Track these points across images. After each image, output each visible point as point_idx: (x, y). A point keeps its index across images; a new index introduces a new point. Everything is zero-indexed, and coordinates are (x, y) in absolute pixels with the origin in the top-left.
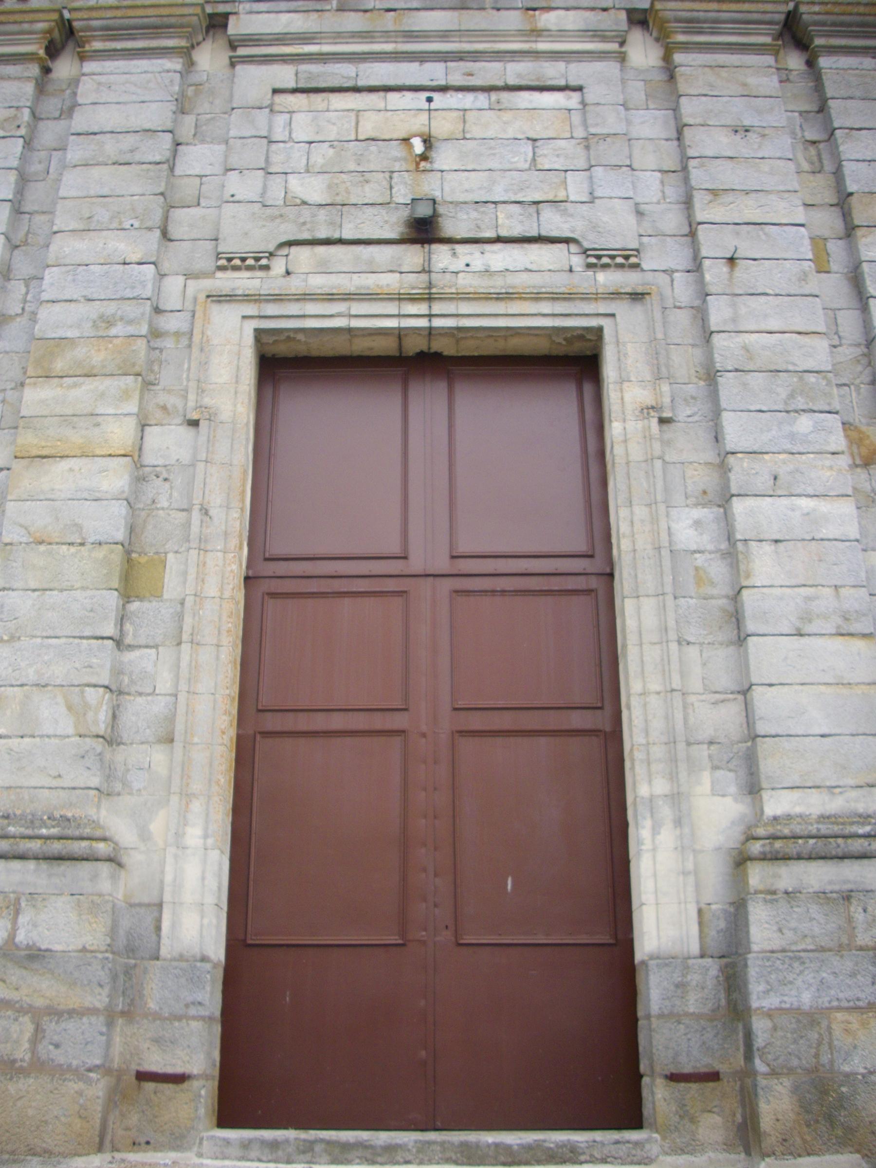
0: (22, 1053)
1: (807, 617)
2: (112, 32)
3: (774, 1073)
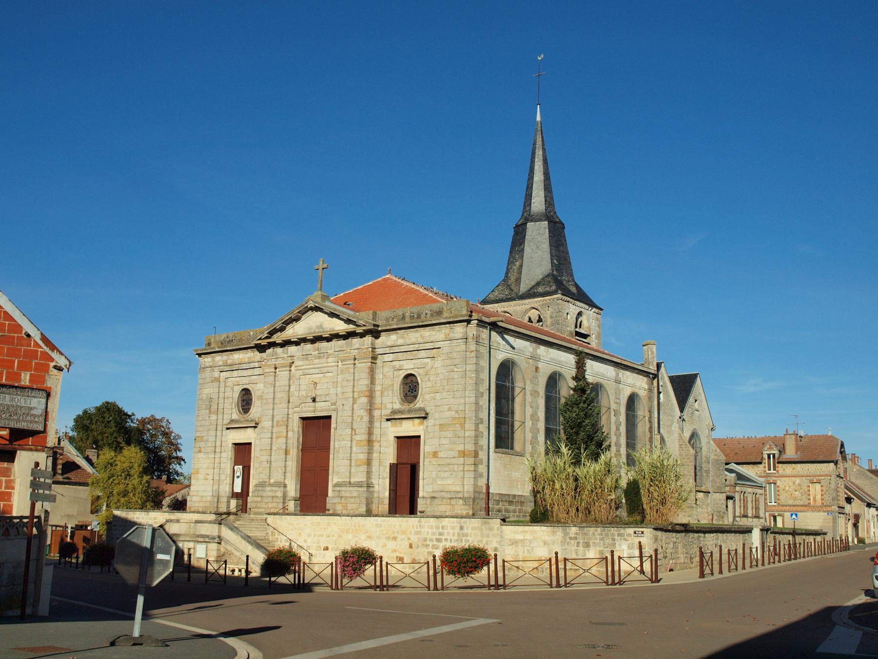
0: (276, 507)
1: (344, 457)
2: (281, 367)
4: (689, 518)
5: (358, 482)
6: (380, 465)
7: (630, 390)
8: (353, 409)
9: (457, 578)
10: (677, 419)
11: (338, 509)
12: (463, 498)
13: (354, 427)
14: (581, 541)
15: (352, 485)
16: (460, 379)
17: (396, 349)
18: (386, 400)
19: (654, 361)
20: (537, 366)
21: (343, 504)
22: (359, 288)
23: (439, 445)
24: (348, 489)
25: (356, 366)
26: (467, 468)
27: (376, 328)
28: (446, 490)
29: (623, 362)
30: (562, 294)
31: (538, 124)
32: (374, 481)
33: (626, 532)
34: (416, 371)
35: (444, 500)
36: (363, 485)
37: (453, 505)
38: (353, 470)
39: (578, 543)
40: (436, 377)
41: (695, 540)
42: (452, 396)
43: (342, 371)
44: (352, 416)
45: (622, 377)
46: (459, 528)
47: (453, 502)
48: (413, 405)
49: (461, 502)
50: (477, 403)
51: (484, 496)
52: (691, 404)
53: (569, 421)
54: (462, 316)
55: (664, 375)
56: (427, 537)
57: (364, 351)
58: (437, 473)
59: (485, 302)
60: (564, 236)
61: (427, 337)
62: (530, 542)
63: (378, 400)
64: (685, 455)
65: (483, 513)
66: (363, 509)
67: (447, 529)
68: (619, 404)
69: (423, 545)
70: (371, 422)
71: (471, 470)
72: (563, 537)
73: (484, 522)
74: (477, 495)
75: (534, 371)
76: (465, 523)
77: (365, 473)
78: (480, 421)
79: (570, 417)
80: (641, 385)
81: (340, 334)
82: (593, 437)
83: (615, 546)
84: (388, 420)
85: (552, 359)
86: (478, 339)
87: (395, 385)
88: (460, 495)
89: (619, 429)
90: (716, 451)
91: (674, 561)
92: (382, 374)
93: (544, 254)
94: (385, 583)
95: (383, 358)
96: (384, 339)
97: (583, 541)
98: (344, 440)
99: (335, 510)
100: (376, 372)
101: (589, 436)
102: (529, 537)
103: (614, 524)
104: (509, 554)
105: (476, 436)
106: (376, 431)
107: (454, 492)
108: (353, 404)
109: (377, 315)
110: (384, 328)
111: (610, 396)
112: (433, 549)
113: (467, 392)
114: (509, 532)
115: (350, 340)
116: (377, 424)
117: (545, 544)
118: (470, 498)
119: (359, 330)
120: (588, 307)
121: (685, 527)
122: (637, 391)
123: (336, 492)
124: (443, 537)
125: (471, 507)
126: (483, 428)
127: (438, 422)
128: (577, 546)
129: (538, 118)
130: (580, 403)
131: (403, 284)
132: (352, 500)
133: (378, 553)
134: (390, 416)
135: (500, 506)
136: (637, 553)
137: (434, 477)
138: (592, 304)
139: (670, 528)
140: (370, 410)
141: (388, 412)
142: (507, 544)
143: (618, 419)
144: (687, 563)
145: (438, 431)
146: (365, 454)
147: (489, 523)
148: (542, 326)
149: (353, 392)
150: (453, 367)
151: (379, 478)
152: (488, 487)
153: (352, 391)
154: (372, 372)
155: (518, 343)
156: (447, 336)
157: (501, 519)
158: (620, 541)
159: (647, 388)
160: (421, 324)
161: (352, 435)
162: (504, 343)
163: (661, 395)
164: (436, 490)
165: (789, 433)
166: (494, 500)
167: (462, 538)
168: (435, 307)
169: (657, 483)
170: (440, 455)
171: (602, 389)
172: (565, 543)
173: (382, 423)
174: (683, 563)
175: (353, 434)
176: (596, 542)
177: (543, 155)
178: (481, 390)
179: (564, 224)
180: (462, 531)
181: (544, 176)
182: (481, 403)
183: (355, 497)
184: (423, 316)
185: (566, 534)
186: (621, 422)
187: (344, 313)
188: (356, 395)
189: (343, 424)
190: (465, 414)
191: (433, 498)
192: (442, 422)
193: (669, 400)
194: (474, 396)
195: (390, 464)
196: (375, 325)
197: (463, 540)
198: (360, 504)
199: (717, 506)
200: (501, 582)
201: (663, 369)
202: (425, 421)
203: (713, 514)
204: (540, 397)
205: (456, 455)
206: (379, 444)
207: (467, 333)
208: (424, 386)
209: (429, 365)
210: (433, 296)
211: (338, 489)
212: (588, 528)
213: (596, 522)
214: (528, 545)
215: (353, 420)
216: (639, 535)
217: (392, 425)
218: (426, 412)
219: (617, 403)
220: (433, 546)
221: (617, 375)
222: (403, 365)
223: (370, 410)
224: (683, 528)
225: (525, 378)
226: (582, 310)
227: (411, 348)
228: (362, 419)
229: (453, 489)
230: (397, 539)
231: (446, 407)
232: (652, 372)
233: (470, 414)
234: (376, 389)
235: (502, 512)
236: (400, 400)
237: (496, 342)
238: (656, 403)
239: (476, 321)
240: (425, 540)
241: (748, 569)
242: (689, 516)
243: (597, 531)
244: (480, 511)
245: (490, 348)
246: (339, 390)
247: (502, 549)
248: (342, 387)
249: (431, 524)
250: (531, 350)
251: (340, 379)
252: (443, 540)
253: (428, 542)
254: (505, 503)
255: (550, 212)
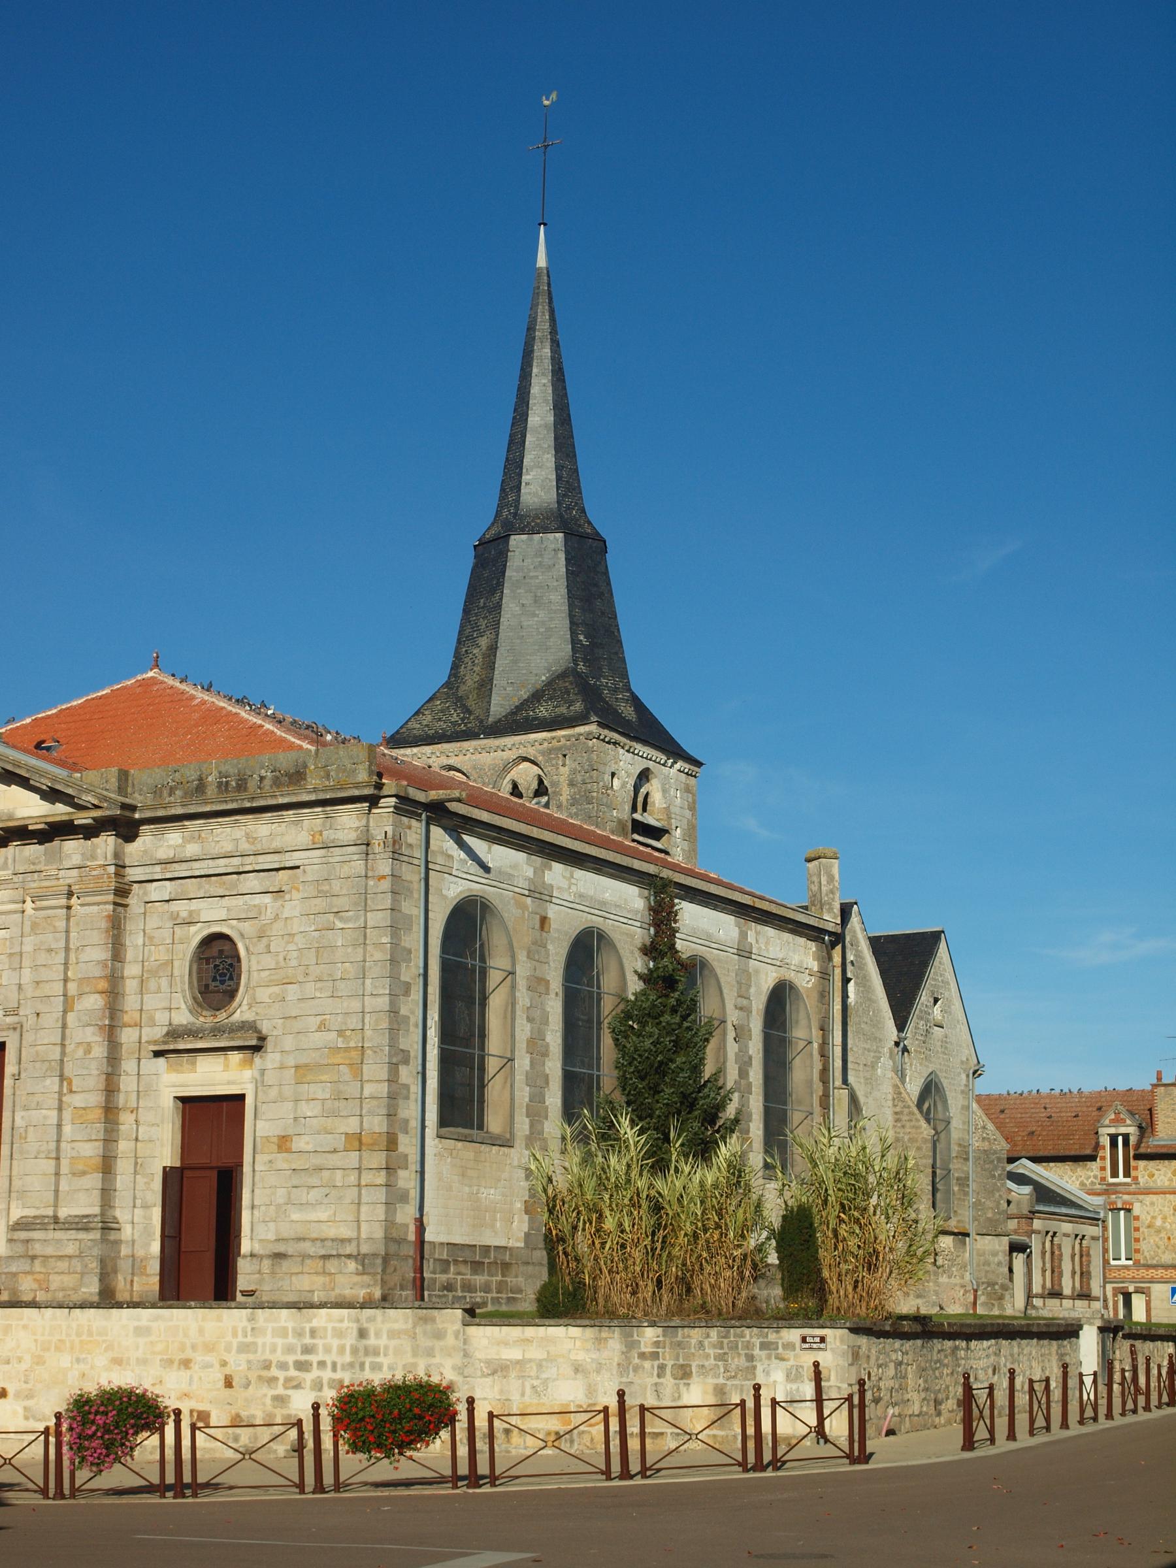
3: (5, 1289)
4: (919, 1301)
5: (76, 1216)
6: (136, 1173)
7: (775, 975)
8: (64, 1026)
9: (373, 1460)
10: (890, 1049)
11: (22, 1288)
12: (358, 1257)
13: (67, 1073)
14: (670, 1363)
15: (61, 1226)
16: (350, 950)
17: (181, 870)
18: (152, 1002)
19: (833, 900)
20: (544, 914)
21: (36, 1276)
22: (75, 703)
23: (295, 1119)
24: (51, 1235)
25: (73, 911)
26: (366, 1178)
27: (128, 814)
28: (314, 1235)
29: (760, 904)
30: (600, 724)
31: (539, 275)
32: (121, 1214)
33: (781, 1338)
34: (232, 927)
35: (308, 1262)
36: (92, 1225)
37: (330, 1274)
38: (64, 1186)
39: (662, 1368)
40: (288, 943)
41: (946, 1357)
42: (330, 994)
43: (34, 926)
44: (63, 1045)
45: (754, 942)
46: (355, 1333)
47: (332, 1266)
48: (224, 1015)
49: (352, 1266)
50: (394, 1011)
51: (410, 1251)
52: (924, 1008)
53: (634, 1059)
54: (357, 786)
55: (858, 933)
56: (271, 1357)
57: (94, 873)
58: (289, 1193)
59: (397, 740)
60: (606, 573)
61: (264, 840)
62: (540, 1366)
63: (131, 1002)
64: (910, 1139)
65: (409, 1293)
66: (91, 1288)
67: (325, 1337)
68: (745, 1010)
69: (260, 1378)
70: (113, 1058)
71: (378, 1183)
72: (623, 1353)
73: (420, 1319)
74: (393, 1248)
75: (537, 926)
76: (371, 1319)
77: (97, 1194)
78: (400, 1057)
79: (636, 1050)
80: (801, 962)
81: (30, 828)
82: (696, 1099)
83: (754, 1374)
84: (158, 1054)
85: (581, 896)
86: (397, 847)
87: (176, 964)
88: (349, 1249)
89: (748, 1074)
90: (984, 1127)
91: (897, 1410)
92: (142, 933)
93: (551, 619)
94: (187, 1478)
95: (145, 894)
96: (146, 842)
97: (672, 1362)
98: (38, 1106)
99: (14, 1292)
100: (128, 928)
101: (684, 1096)
102: (535, 1353)
103: (751, 1319)
104: (485, 1399)
105: (392, 1097)
106: (127, 1084)
107: (333, 1240)
108: (65, 1012)
109: (130, 778)
110: (148, 814)
111: (725, 991)
112: (286, 1388)
113: (368, 982)
114: (485, 1342)
115: (56, 843)
116: (128, 1065)
117: (577, 1371)
118: (375, 1255)
119: (83, 819)
120: (664, 758)
121: (923, 1325)
122: (791, 976)
123: (19, 1244)
124: (313, 1359)
125: (379, 1277)
126: (407, 1075)
127: (291, 1061)
128: (659, 1376)
129: (542, 261)
130: (662, 1013)
131: (193, 697)
132: (63, 1265)
133: (170, 1402)
134: (165, 1043)
135: (451, 1276)
136: (809, 1391)
137: (281, 1201)
138: (674, 751)
139: (888, 1328)
140: (112, 1028)
141: (159, 1032)
142: (479, 1373)
143: (743, 1050)
144: (926, 1413)
145: (293, 1082)
146: (97, 1144)
147: (433, 1320)
148: (547, 806)
149: (66, 980)
150: (331, 917)
151: (134, 1207)
152: (421, 1228)
153: (62, 977)
154: (116, 928)
155: (498, 855)
156: (317, 836)
157: (465, 1310)
158: (767, 1362)
159: (816, 969)
160: (248, 805)
161: (61, 1093)
162: (463, 855)
163: (851, 987)
164: (285, 1235)
165: (1165, 1081)
166: (435, 1260)
167: (362, 1359)
168: (285, 760)
169: (856, 1214)
170: (300, 1144)
171: (706, 972)
172: (628, 1368)
173: (143, 1061)
174: (918, 1416)
175: (65, 1091)
176: (706, 1363)
177: (553, 358)
178: (405, 977)
179: (605, 542)
180: (364, 1342)
181: (555, 415)
182: (403, 1011)
183: (70, 1257)
184: (252, 784)
185: (631, 1345)
186: (750, 1058)
187: (42, 773)
188: (72, 988)
189: (38, 1065)
190: (363, 1038)
191: (279, 1256)
192: (303, 1060)
193: (870, 1000)
194: (388, 992)
195: (165, 1168)
196: (124, 806)
197: (367, 1366)
198: (82, 1274)
199: (987, 1268)
200: (483, 1468)
201: (855, 920)
202: (257, 1059)
203: (976, 1291)
204: (552, 995)
205: (340, 1142)
206: (133, 1117)
207: (368, 830)
208: (254, 967)
209: (269, 910)
210: (276, 730)
211: (23, 1235)
212: (686, 1330)
213: (707, 1315)
214: (533, 1373)
215: (63, 1053)
216: (815, 1346)
217: (171, 1069)
218: (259, 1032)
219: (741, 1009)
220: (288, 1380)
221: (743, 935)
222: (198, 912)
223: (112, 1028)
224: (918, 1328)
225: (515, 944)
226: (651, 764)
227: (221, 866)
228: (88, 1051)
229: (332, 1232)
230: (192, 1365)
231: (314, 1022)
232: (830, 927)
233: (376, 1036)
234: (126, 973)
235: (456, 1291)
236: (190, 1002)
237: (442, 853)
238: (838, 1007)
239: (394, 799)
240: (267, 1366)
241: (1075, 1429)
242: (918, 1296)
243: (708, 1336)
244: (402, 1288)
245: (427, 869)
246: (27, 976)
247: (466, 1387)
248: (35, 968)
249: (283, 1324)
250: (530, 873)
251: (28, 948)
252: (315, 1365)
253: (274, 1372)
254: (462, 1268)
255: (569, 508)
